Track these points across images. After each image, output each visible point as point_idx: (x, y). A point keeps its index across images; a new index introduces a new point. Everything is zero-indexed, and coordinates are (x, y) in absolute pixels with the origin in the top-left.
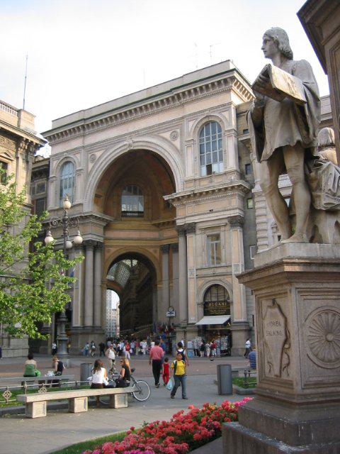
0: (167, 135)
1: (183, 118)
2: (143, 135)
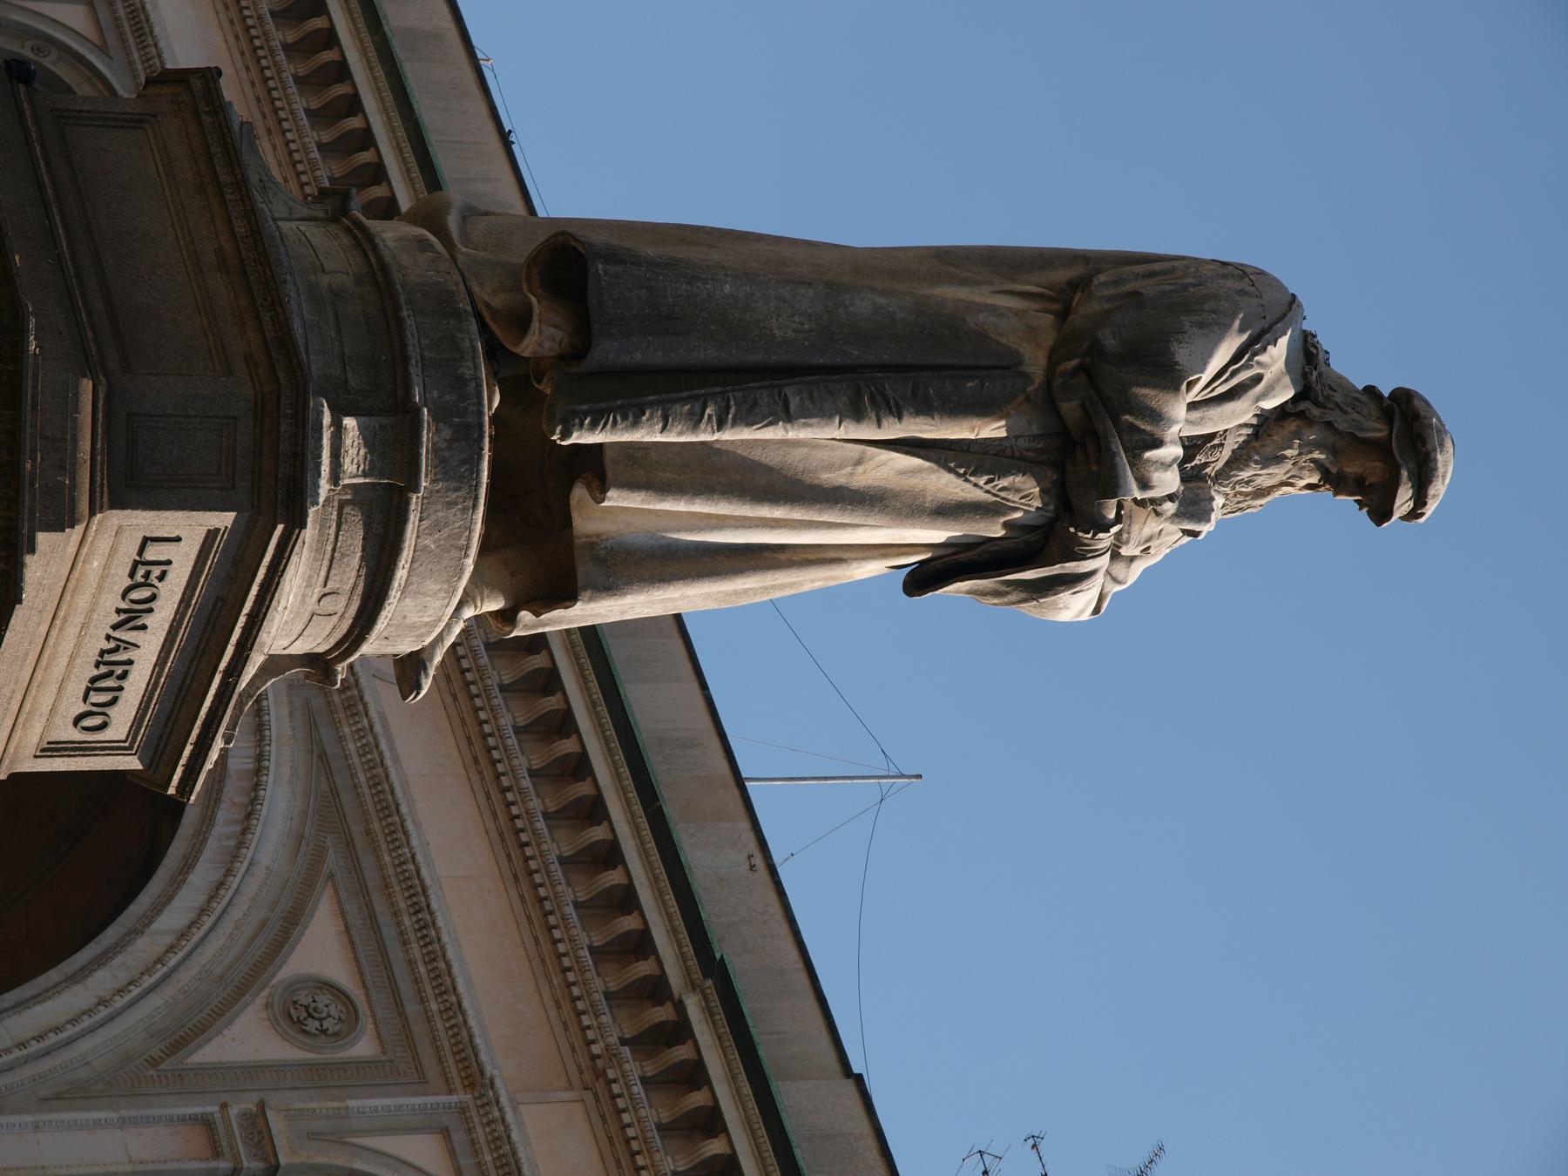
0: (320, 952)
1: (475, 1078)
2: (320, 759)
